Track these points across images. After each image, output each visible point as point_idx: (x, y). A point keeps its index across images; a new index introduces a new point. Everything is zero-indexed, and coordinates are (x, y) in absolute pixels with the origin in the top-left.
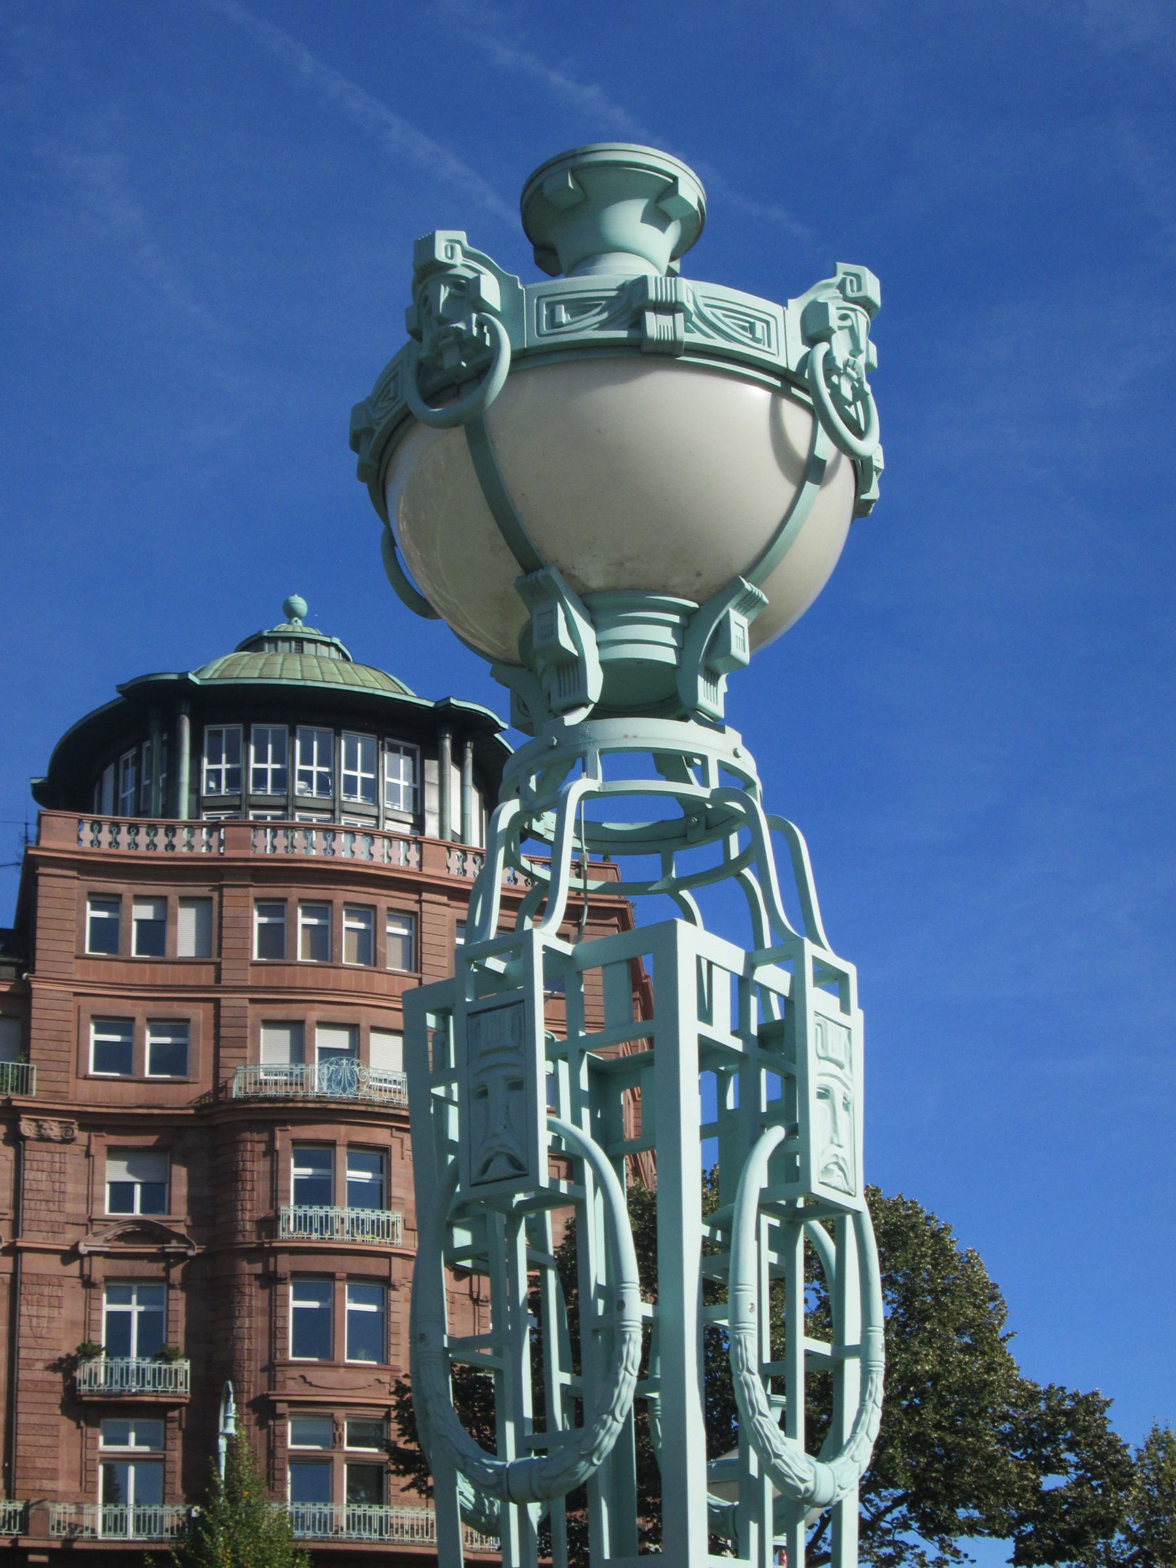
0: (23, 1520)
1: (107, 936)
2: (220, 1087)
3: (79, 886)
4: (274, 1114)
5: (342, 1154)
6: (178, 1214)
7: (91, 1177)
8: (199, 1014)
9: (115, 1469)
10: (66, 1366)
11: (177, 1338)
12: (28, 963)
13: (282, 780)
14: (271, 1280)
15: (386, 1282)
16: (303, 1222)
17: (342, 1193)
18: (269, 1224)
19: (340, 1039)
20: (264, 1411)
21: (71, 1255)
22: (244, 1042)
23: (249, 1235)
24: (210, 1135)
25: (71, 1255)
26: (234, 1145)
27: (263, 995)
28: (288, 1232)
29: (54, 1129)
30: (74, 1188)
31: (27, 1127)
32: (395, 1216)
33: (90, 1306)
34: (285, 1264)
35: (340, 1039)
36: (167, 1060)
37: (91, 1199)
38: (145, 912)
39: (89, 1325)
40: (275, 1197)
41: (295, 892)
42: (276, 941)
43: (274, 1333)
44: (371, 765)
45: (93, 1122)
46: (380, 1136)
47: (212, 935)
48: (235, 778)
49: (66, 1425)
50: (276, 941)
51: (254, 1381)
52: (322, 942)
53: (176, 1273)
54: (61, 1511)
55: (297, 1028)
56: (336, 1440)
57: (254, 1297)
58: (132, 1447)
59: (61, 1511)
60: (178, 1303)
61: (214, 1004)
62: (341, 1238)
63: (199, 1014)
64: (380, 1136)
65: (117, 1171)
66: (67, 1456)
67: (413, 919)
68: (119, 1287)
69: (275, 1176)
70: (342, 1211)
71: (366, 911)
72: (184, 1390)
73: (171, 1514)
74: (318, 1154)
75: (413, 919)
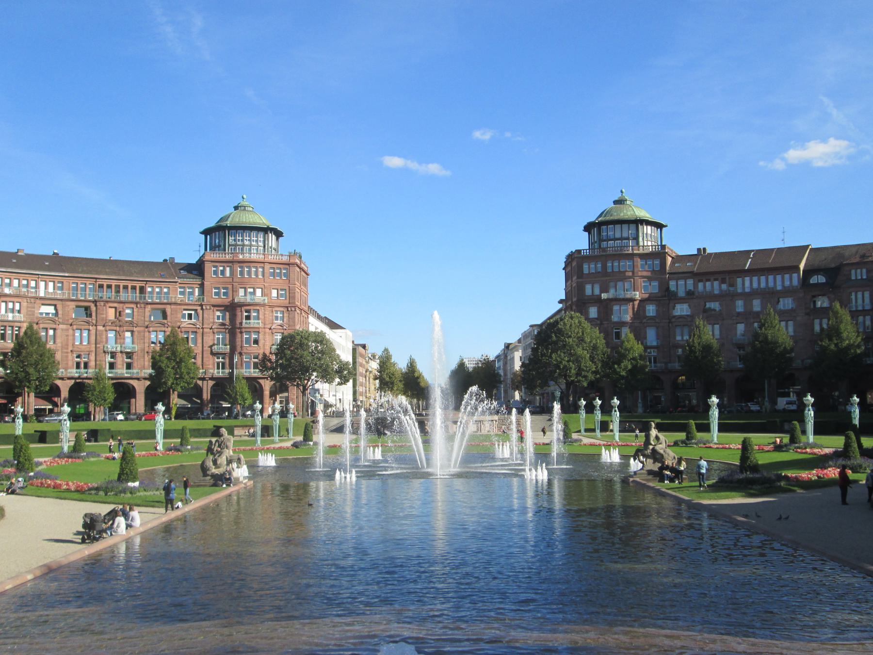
1: (215, 273)
2: (233, 299)
6: (228, 320)
7: (214, 314)
9: (218, 364)
10: (211, 347)
11: (228, 342)
12: (203, 279)
13: (242, 240)
14: (241, 333)
17: (252, 317)
18: (241, 323)
19: (251, 290)
20: (241, 354)
22: (237, 291)
23: (238, 326)
24: (232, 308)
26: (236, 310)
27: (240, 283)
28: (244, 325)
30: (211, 317)
35: (251, 290)
36: (225, 294)
38: (221, 268)
43: (242, 341)
44: (257, 237)
45: (214, 306)
46: (258, 308)
47: (232, 272)
48: (235, 240)
50: (242, 273)
51: (239, 349)
52: (249, 273)
55: (245, 289)
57: (239, 335)
59: (211, 371)
60: (228, 335)
61: (232, 285)
62: (252, 326)
63: (230, 287)
64: (258, 308)
65: (218, 313)
66: (211, 362)
67: (263, 268)
68: (219, 333)
70: (252, 321)
73: (227, 371)
74: (248, 311)
75: (263, 268)
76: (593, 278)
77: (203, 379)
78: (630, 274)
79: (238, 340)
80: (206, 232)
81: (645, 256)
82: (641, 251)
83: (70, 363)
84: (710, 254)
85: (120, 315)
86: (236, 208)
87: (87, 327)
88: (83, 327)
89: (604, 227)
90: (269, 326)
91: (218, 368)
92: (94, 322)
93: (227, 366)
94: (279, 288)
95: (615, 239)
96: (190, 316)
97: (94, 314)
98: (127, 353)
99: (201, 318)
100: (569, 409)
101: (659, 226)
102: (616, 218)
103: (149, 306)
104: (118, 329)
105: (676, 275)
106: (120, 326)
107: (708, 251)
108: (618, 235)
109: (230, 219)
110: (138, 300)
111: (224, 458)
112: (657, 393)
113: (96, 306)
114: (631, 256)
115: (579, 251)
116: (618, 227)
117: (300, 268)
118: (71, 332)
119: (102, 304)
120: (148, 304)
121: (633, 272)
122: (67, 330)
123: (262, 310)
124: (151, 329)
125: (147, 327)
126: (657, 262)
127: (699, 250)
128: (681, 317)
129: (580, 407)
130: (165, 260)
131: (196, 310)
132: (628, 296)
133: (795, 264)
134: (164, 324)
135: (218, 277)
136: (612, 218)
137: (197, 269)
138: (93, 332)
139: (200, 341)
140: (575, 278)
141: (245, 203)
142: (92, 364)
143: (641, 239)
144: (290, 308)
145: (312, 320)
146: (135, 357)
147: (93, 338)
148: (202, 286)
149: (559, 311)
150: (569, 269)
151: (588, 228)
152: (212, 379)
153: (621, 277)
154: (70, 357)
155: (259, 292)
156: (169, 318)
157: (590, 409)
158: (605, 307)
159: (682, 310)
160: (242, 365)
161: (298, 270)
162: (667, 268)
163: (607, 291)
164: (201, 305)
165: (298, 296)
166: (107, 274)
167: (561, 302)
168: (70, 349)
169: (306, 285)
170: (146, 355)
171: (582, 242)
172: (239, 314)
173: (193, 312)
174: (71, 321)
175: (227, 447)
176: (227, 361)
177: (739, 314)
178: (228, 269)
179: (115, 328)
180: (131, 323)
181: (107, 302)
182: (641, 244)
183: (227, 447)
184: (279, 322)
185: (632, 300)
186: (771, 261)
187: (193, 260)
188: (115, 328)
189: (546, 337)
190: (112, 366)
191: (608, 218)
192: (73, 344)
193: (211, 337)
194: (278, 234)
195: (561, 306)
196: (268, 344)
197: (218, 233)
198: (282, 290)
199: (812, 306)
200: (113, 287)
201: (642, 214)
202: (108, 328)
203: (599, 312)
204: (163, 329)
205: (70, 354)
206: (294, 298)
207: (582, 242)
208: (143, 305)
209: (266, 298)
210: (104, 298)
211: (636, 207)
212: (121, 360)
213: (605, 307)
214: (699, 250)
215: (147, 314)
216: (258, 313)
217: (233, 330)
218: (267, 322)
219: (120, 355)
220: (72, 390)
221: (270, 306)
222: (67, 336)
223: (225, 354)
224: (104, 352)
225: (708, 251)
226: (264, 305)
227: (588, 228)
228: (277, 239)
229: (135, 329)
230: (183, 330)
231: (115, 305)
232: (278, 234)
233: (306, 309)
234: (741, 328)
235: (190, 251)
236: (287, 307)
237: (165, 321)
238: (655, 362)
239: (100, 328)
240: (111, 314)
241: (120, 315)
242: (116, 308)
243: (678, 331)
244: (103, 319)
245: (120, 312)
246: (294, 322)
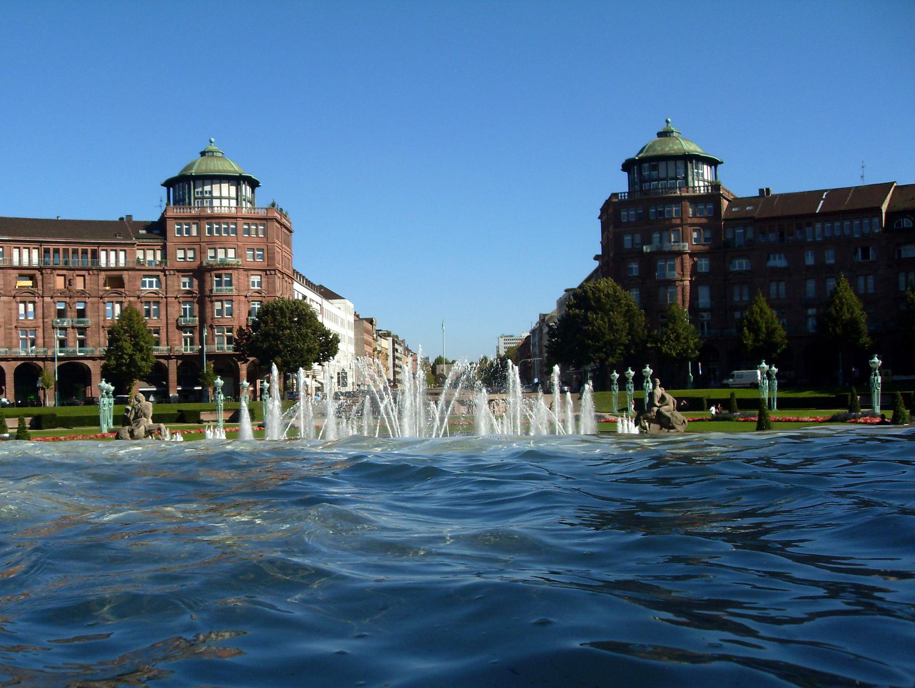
0: (170, 350)
1: (180, 231)
2: (202, 263)
3: (174, 221)
4: (210, 269)
5: (223, 276)
7: (179, 281)
8: (197, 247)
11: (196, 313)
14: (212, 302)
15: (232, 301)
16: (217, 290)
18: (211, 291)
20: (211, 327)
21: (176, 298)
23: (208, 293)
25: (176, 298)
29: (172, 272)
30: (176, 284)
31: (167, 273)
32: (233, 287)
33: (180, 307)
34: (214, 299)
37: (179, 286)
39: (180, 311)
40: (212, 285)
41: (213, 221)
42: (210, 231)
43: (213, 312)
45: (179, 271)
46: (230, 272)
49: (177, 331)
50: (210, 231)
51: (209, 321)
53: (195, 300)
54: (176, 348)
56: (223, 332)
57: (209, 305)
58: (188, 334)
60: (196, 306)
66: (177, 337)
68: (185, 303)
69: (212, 281)
71: (227, 224)
72: (197, 323)
77: (168, 358)
78: (678, 221)
79: (208, 310)
80: (169, 184)
81: (696, 200)
82: (691, 194)
83: (14, 341)
84: (775, 196)
85: (70, 285)
86: (203, 154)
87: (32, 299)
88: (28, 299)
89: (646, 165)
90: (244, 294)
91: (186, 344)
92: (40, 292)
93: (197, 340)
94: (255, 247)
95: (659, 180)
96: (151, 284)
97: (40, 283)
98: (79, 328)
99: (164, 286)
100: (602, 386)
101: (713, 163)
102: (660, 153)
103: (103, 273)
104: (68, 300)
105: (733, 221)
106: (70, 297)
108: (662, 174)
109: (195, 167)
110: (90, 265)
111: (142, 428)
112: (705, 365)
113: (42, 274)
114: (680, 199)
115: (615, 195)
117: (280, 224)
118: (14, 305)
119: (49, 271)
121: (682, 221)
122: (10, 302)
123: (235, 274)
124: (106, 300)
125: (101, 298)
126: (710, 206)
127: (761, 191)
128: (739, 273)
129: (612, 381)
130: (121, 219)
131: (157, 277)
132: (676, 248)
133: (876, 205)
134: (120, 294)
135: (182, 236)
136: (655, 153)
137: (158, 229)
138: (39, 304)
139: (163, 313)
140: (611, 228)
141: (213, 148)
142: (40, 341)
143: (690, 178)
144: (268, 271)
145: (296, 286)
146: (88, 332)
147: (40, 311)
148: (164, 249)
150: (605, 217)
151: (628, 166)
152: (178, 357)
153: (666, 226)
154: (14, 335)
155: (231, 253)
156: (126, 286)
157: (623, 381)
158: (649, 262)
159: (740, 265)
160: (213, 340)
161: (278, 226)
162: (723, 213)
163: (649, 242)
164: (163, 271)
165: (278, 257)
166: (53, 236)
167: (597, 258)
168: (14, 324)
169: (289, 244)
170: (101, 330)
171: (620, 184)
172: (208, 279)
173: (154, 280)
174: (13, 293)
175: (145, 416)
176: (197, 336)
177: (809, 268)
178: (194, 227)
179: (64, 299)
180: (83, 292)
181: (55, 269)
182: (691, 184)
183: (145, 416)
184: (256, 288)
185: (680, 253)
186: (846, 205)
187: (156, 218)
188: (64, 299)
189: (579, 301)
190: (63, 343)
191: (650, 154)
192: (18, 320)
193: (177, 308)
194: (254, 184)
196: (244, 314)
197: (181, 186)
198: (259, 250)
199: (896, 257)
200: (61, 251)
201: (691, 147)
202: (56, 299)
203: (640, 268)
204: (120, 299)
205: (14, 331)
206: (273, 258)
207: (620, 184)
208: (95, 272)
209: (240, 260)
210: (51, 265)
211: (684, 139)
212: (73, 337)
213: (649, 262)
214: (761, 191)
215: (102, 282)
216: (231, 278)
217: (202, 299)
218: (242, 289)
219: (71, 330)
220: (18, 372)
221: (245, 270)
222: (10, 309)
223: (194, 327)
224: (53, 328)
225: (773, 192)
226: (236, 268)
227: (628, 166)
228: (253, 192)
229: (87, 300)
230: (144, 300)
231: (64, 272)
232: (254, 184)
233: (290, 273)
234: (811, 285)
235: (149, 206)
236: (265, 271)
237: (123, 290)
238: (709, 328)
239: (47, 299)
240: (60, 283)
241: (70, 285)
242: (64, 275)
243: (736, 290)
244: (50, 289)
245: (70, 281)
246: (274, 287)
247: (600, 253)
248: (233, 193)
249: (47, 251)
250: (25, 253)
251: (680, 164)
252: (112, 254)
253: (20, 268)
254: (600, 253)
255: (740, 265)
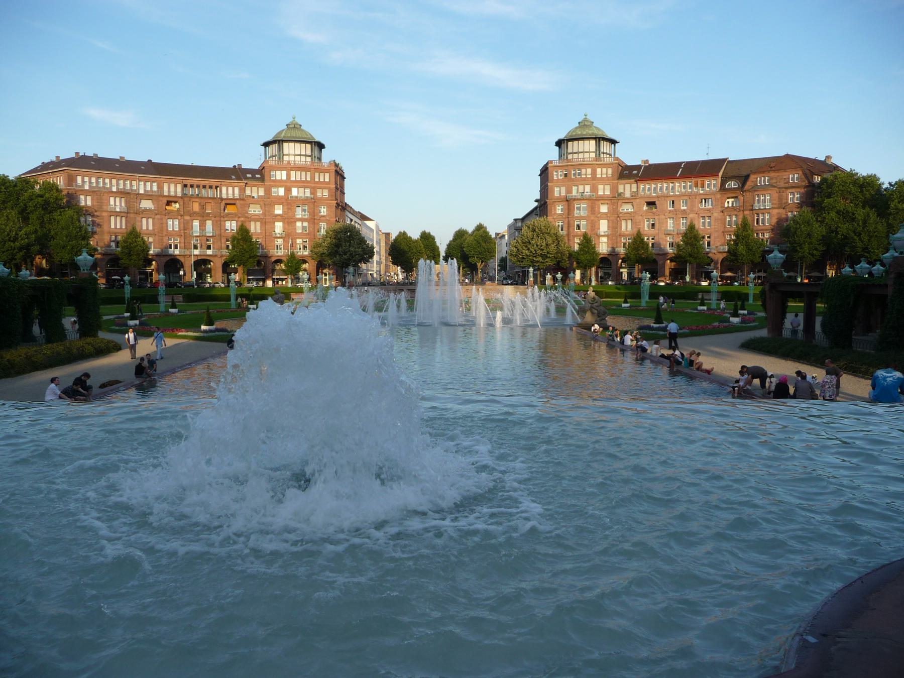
76: (560, 183)
101: (613, 142)
107: (651, 162)
115: (551, 162)
116: (581, 142)
120: (222, 199)
149: (536, 208)
151: (559, 143)
167: (536, 201)
171: (553, 154)
195: (536, 204)
227: (559, 143)
232: (321, 146)
240: (196, 207)
243: (624, 223)
247: (539, 198)
248: (309, 153)
249: (185, 186)
250: (172, 186)
251: (593, 142)
252: (230, 189)
253: (169, 196)
254: (539, 198)
255: (627, 208)
